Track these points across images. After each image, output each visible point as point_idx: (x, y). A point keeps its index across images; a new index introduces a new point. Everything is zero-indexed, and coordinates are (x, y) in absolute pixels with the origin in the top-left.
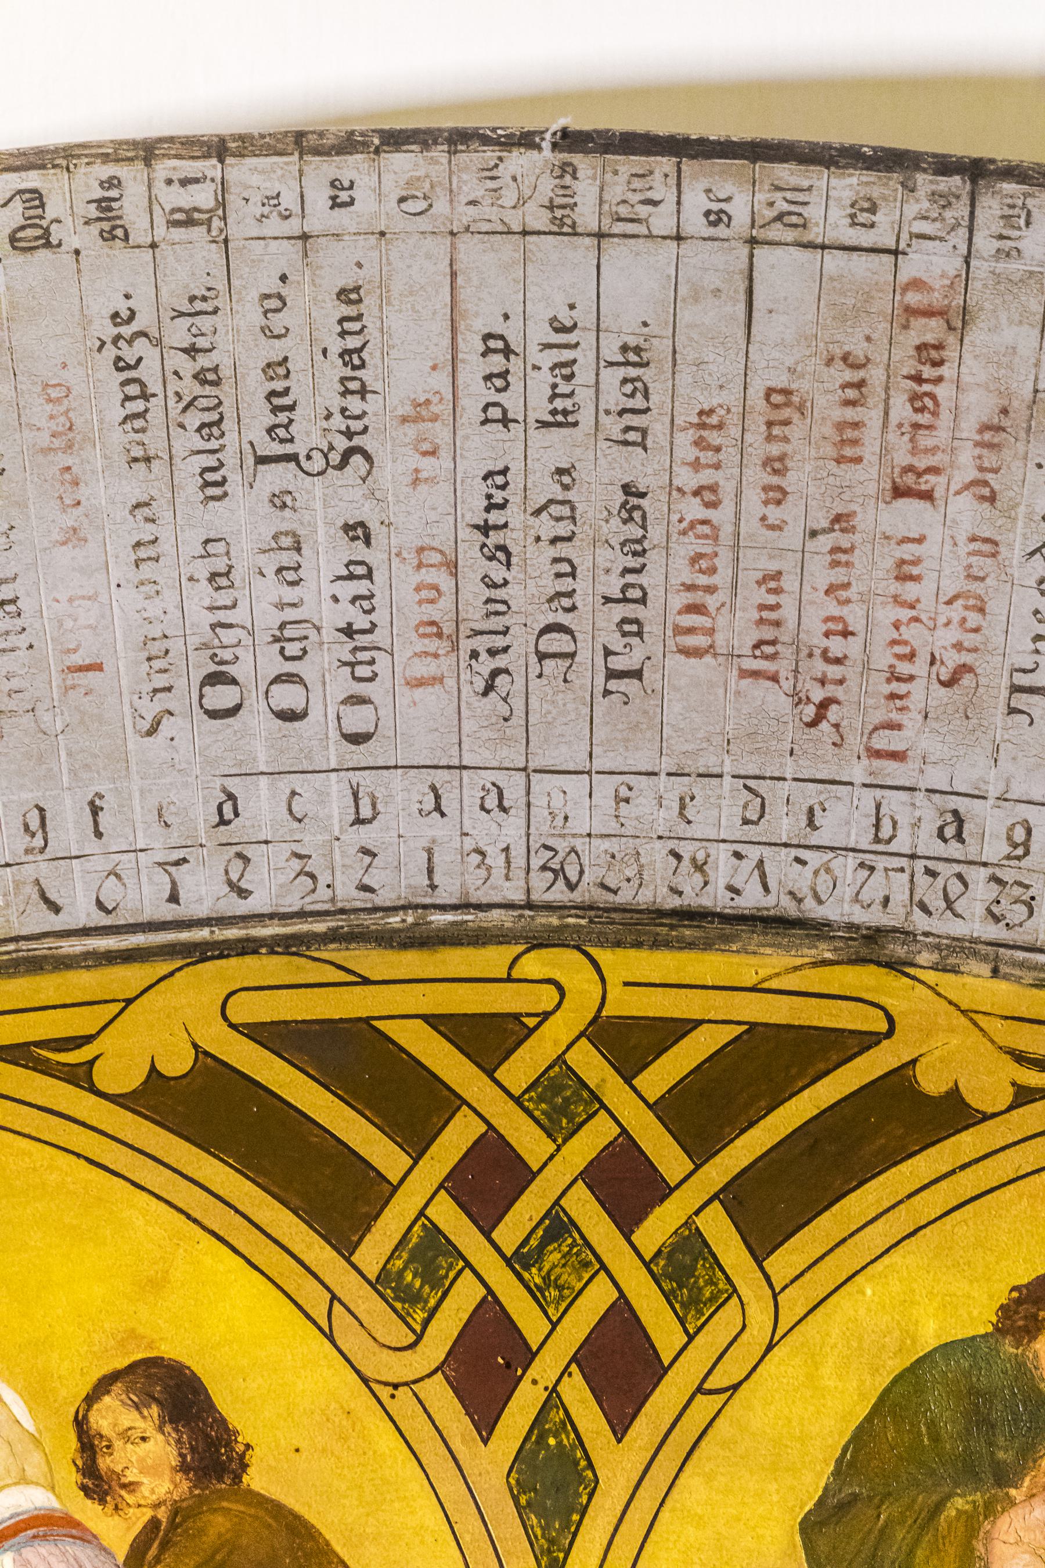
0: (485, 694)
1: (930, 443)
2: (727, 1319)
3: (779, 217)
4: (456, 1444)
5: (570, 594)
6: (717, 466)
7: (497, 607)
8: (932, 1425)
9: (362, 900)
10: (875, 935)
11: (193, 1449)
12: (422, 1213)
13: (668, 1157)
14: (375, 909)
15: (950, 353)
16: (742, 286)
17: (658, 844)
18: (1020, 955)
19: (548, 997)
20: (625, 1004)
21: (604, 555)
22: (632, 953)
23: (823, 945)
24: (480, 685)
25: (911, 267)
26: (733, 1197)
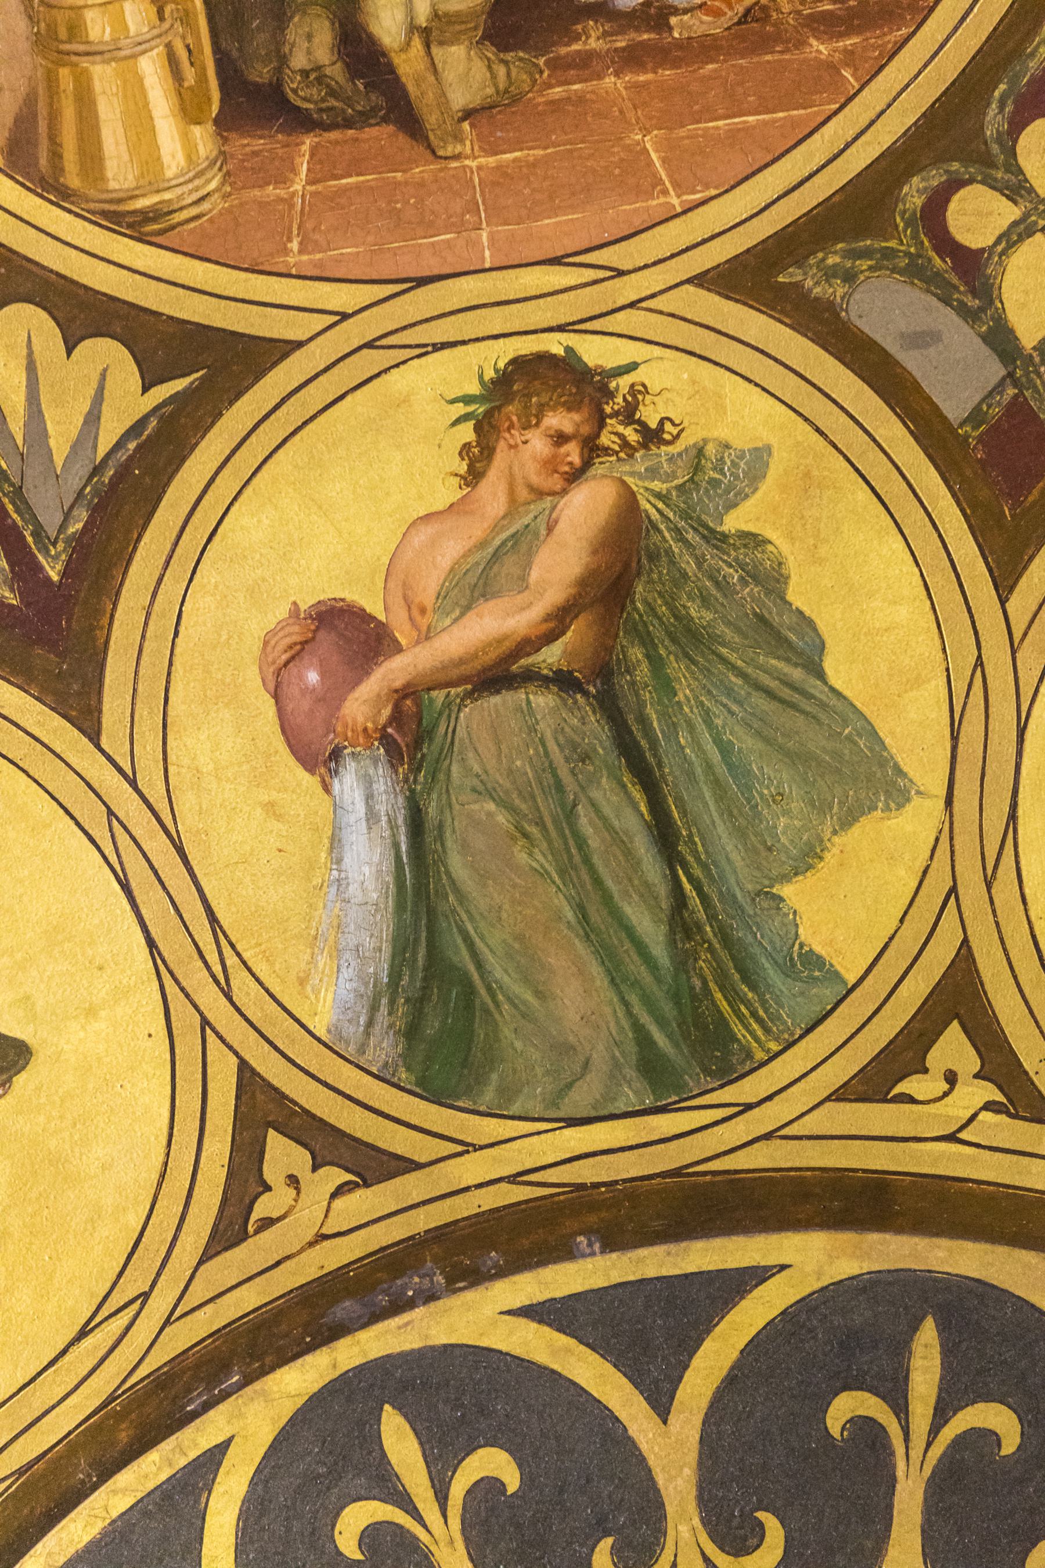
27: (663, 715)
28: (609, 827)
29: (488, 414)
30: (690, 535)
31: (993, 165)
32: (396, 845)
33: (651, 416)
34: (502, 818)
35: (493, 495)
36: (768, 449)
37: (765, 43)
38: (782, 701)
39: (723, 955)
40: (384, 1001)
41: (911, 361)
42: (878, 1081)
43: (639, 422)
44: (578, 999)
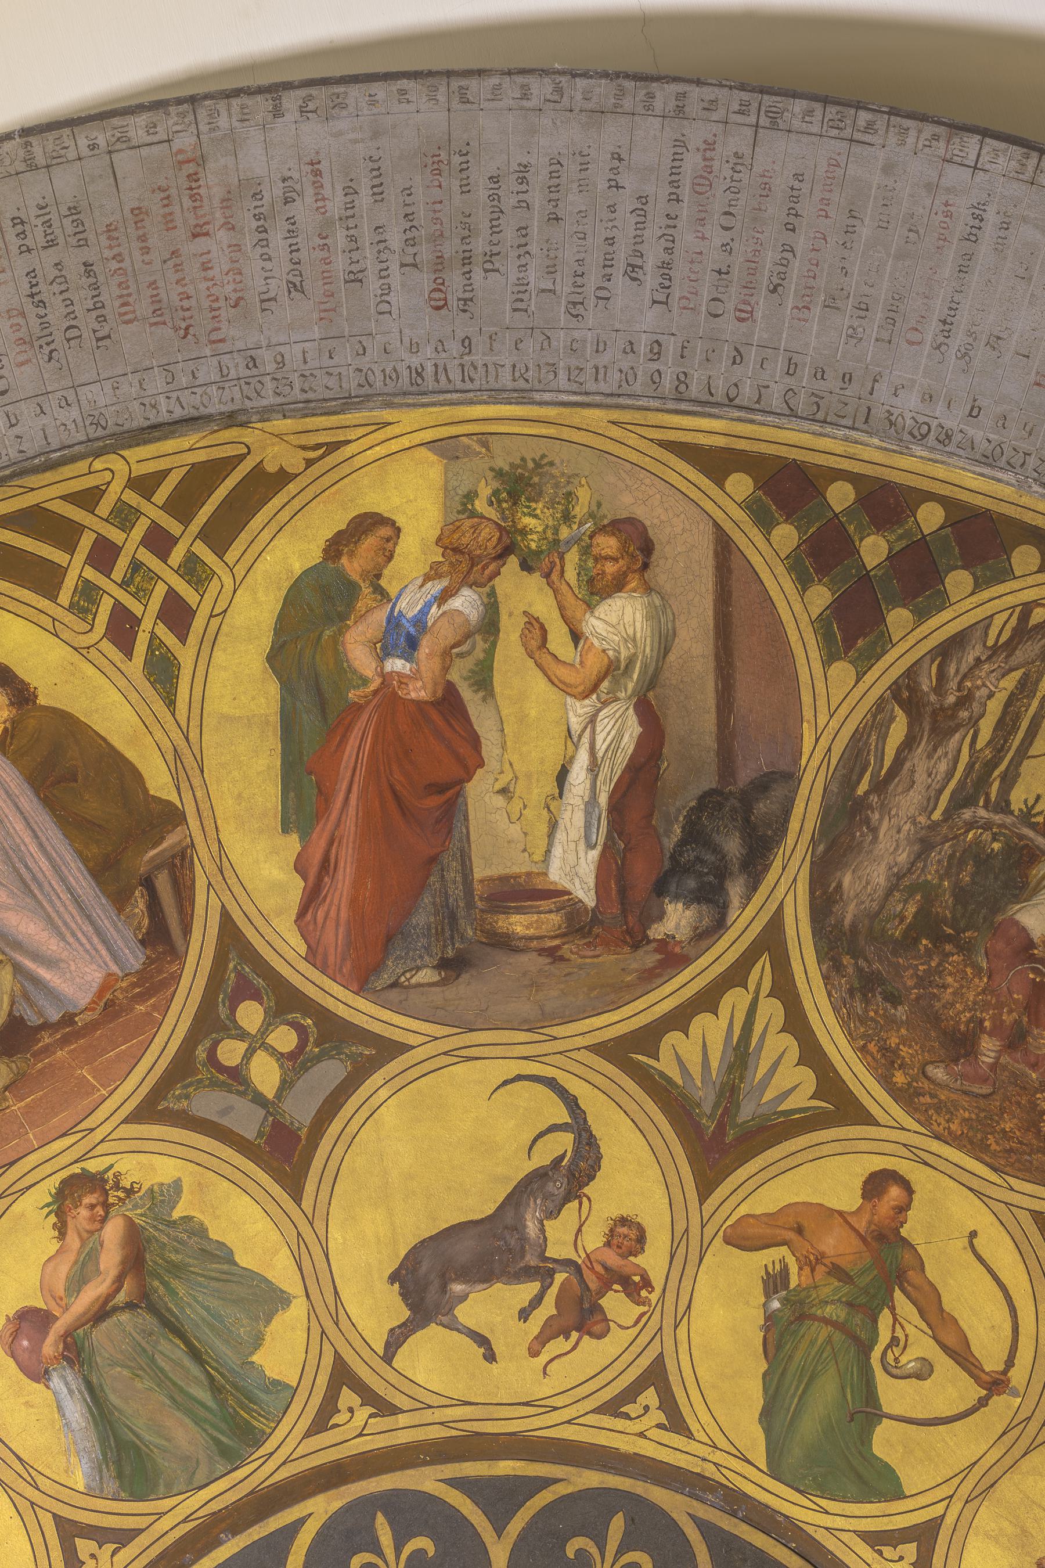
0: (49, 361)
1: (202, 213)
2: (215, 584)
3: (118, 140)
4: (119, 664)
5: (73, 312)
6: (119, 245)
7: (45, 325)
8: (308, 605)
9: (21, 457)
10: (231, 415)
11: (14, 696)
12: (80, 576)
13: (174, 527)
14: (28, 459)
15: (201, 175)
16: (110, 171)
17: (135, 402)
18: (292, 406)
19: (108, 476)
20: (139, 470)
21: (82, 293)
22: (137, 449)
23: (212, 424)
24: (46, 358)
25: (176, 145)
26: (203, 535)
27: (176, 1305)
28: (171, 1360)
29: (59, 1207)
30: (160, 1227)
31: (229, 1030)
32: (85, 1400)
33: (126, 1183)
34: (125, 1372)
35: (73, 1240)
36: (179, 1179)
37: (117, 1015)
38: (223, 1281)
39: (238, 1395)
40: (104, 1467)
41: (225, 1122)
42: (321, 1424)
43: (123, 1188)
44: (184, 1436)
